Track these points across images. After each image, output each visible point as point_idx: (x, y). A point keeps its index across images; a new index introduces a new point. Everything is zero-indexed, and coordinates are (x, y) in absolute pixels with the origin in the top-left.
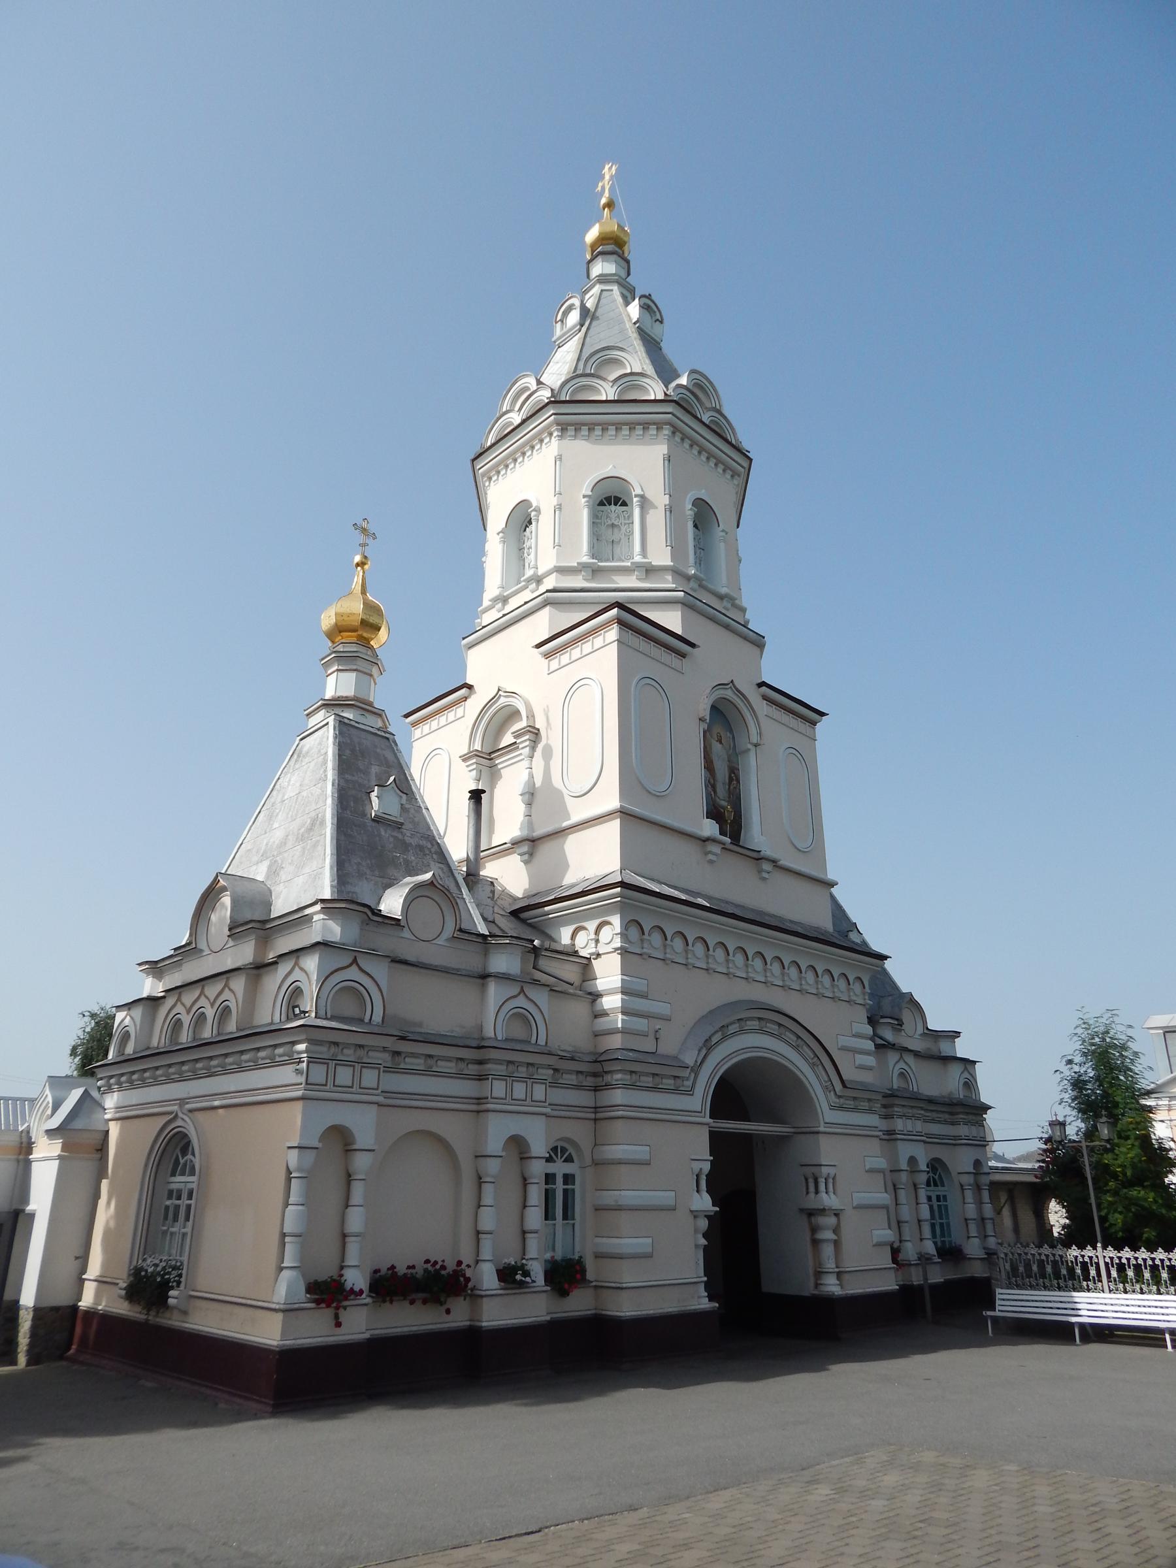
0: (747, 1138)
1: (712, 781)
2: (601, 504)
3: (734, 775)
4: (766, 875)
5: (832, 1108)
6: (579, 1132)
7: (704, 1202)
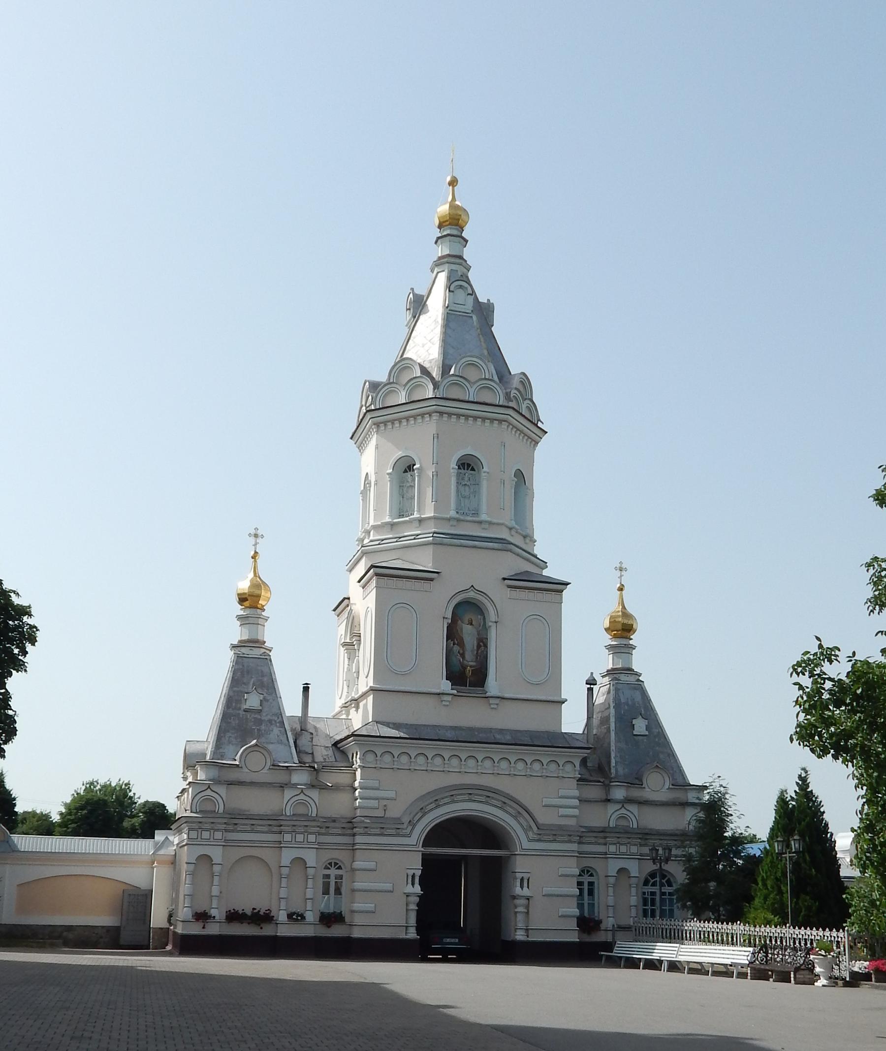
0: (499, 858)
1: (461, 652)
2: (405, 471)
3: (482, 643)
4: (495, 706)
5: (530, 840)
6: (342, 856)
7: (417, 889)
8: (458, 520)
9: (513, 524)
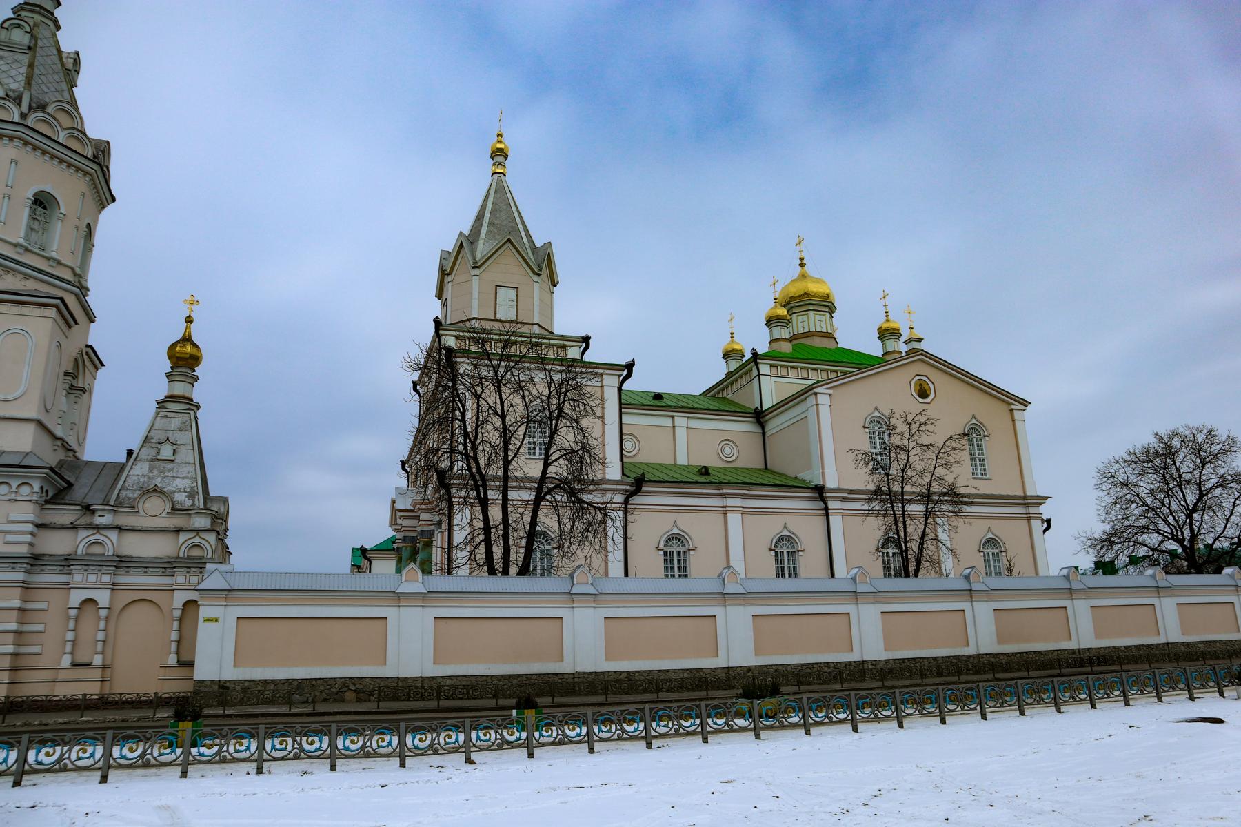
8: (27, 250)
9: (78, 271)
